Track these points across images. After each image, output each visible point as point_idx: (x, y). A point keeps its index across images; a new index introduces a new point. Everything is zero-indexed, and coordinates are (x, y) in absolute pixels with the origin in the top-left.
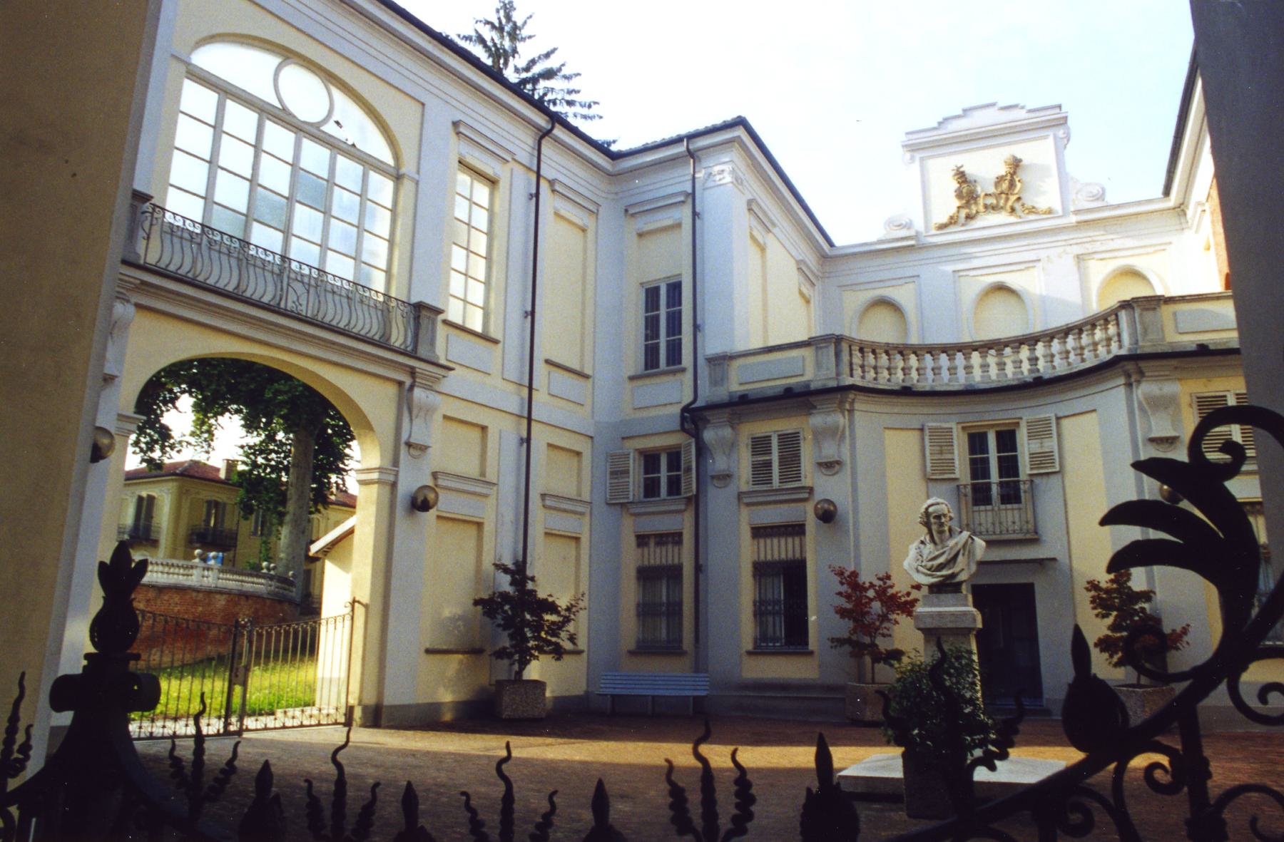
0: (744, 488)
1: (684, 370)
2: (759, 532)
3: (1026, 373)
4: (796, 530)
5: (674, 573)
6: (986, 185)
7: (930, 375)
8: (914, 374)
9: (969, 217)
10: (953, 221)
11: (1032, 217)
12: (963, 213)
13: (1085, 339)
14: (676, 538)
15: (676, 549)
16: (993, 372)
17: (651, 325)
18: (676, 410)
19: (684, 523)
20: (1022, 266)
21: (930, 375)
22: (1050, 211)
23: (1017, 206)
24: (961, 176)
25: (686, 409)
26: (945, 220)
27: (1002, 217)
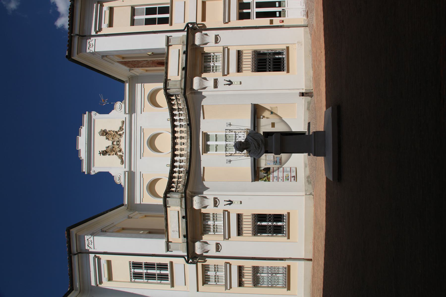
0: (222, 238)
1: (171, 263)
2: (239, 233)
3: (186, 129)
4: (239, 216)
5: (256, 270)
6: (109, 143)
7: (182, 164)
8: (182, 169)
9: (120, 151)
10: (121, 157)
11: (124, 127)
12: (119, 153)
13: (175, 107)
14: (240, 268)
15: (246, 269)
16: (184, 141)
17: (150, 277)
18: (188, 265)
19: (235, 264)
20: (142, 133)
21: (182, 164)
22: (123, 122)
23: (119, 133)
24: (104, 153)
25: (187, 262)
26: (120, 160)
27: (122, 139)
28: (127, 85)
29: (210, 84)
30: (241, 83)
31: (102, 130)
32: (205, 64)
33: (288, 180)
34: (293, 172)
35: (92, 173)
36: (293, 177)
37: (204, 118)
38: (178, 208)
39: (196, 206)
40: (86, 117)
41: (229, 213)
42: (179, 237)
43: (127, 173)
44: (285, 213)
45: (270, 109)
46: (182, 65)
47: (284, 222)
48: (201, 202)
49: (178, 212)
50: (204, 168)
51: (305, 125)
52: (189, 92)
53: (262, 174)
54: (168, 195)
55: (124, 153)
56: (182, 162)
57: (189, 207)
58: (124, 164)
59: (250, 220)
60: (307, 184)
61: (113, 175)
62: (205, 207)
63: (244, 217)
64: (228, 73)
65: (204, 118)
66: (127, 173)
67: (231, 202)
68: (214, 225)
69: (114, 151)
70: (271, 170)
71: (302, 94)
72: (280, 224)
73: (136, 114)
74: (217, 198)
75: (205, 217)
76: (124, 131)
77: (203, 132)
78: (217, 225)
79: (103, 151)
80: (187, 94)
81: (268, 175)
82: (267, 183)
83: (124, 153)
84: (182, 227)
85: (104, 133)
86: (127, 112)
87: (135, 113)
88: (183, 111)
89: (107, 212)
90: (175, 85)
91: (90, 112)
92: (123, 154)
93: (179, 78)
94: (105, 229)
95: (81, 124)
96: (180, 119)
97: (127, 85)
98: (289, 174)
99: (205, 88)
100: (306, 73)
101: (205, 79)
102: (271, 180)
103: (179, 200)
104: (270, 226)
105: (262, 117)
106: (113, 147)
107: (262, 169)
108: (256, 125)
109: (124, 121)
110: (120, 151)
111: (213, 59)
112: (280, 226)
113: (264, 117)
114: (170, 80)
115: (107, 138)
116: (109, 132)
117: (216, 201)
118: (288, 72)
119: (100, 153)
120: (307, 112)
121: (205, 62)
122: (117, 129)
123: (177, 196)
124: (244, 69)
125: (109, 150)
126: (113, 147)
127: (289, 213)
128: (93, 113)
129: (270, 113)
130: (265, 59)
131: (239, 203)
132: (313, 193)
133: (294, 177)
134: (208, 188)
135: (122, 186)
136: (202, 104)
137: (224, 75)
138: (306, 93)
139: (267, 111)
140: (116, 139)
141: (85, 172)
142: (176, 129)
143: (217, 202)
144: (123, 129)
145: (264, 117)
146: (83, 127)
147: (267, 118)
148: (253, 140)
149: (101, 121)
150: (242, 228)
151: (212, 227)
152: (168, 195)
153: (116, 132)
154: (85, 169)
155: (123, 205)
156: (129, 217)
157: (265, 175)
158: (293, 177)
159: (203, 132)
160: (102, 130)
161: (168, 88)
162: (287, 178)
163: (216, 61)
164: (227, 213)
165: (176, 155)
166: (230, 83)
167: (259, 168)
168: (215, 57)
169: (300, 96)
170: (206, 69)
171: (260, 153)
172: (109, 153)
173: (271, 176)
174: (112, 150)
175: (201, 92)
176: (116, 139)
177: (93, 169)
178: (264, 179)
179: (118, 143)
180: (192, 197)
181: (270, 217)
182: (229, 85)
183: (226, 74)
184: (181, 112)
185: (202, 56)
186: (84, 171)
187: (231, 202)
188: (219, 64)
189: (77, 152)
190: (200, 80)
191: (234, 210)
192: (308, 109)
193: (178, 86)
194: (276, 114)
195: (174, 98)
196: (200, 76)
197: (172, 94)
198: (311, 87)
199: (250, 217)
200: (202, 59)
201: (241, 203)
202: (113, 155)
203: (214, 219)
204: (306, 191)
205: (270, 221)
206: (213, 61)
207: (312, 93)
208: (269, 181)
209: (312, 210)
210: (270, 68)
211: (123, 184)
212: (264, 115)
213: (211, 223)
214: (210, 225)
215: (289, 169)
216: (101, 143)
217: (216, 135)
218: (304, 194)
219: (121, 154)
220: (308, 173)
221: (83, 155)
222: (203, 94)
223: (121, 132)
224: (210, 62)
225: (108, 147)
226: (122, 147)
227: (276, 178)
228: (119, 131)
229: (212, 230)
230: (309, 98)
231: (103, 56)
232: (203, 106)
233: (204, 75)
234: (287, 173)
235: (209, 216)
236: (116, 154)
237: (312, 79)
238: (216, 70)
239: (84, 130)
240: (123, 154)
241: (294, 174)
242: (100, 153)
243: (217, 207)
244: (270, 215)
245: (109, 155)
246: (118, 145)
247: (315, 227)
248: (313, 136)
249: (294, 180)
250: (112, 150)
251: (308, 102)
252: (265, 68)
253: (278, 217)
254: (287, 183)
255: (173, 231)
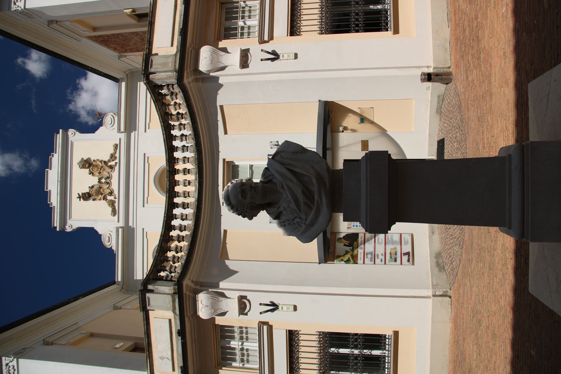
4: (292, 337)
6: (94, 181)
8: (184, 233)
9: (111, 193)
10: (112, 204)
11: (117, 155)
12: (109, 198)
22: (116, 146)
23: (110, 164)
24: (86, 197)
27: (115, 174)
28: (123, 84)
29: (234, 59)
30: (296, 56)
31: (83, 159)
32: (228, 24)
33: (396, 261)
34: (406, 243)
35: (68, 229)
36: (405, 254)
37: (226, 133)
38: (170, 314)
39: (203, 313)
40: (59, 138)
41: (270, 328)
42: (174, 370)
43: (120, 230)
44: (389, 333)
45: (358, 111)
46: (179, 26)
47: (385, 349)
48: (214, 306)
49: (170, 320)
50: (225, 231)
51: (430, 145)
52: (190, 79)
53: (340, 247)
54: (150, 287)
55: (117, 197)
56: (184, 218)
57: (188, 313)
58: (117, 216)
59: (315, 344)
60: (436, 270)
61: (100, 233)
62: (223, 314)
63: (302, 337)
64: (271, 38)
65: (226, 133)
66: (120, 230)
67: (274, 307)
68: (242, 349)
69: (102, 194)
70: (360, 239)
71: (429, 77)
72: (376, 352)
73: (136, 132)
74: (245, 297)
75: (225, 333)
76: (117, 161)
77: (224, 160)
78: (247, 350)
79: (84, 194)
80: (186, 81)
81: (353, 250)
82: (351, 266)
83: (117, 197)
84: (178, 351)
85: (87, 164)
86: (122, 129)
87: (135, 130)
88: (186, 119)
89: (76, 299)
90: (165, 64)
91: (66, 130)
92: (115, 198)
93: (174, 50)
94: (50, 340)
95: (51, 150)
96: (182, 135)
97: (123, 84)
98: (398, 247)
99: (223, 68)
100: (436, 33)
101: (225, 50)
102: (360, 261)
103: (169, 298)
104: (356, 357)
105: (341, 129)
106: (100, 188)
107: (342, 235)
108: (329, 145)
109: (117, 145)
110: (111, 193)
111: (243, 12)
112: (377, 358)
113: (345, 128)
114: (157, 54)
115: (91, 173)
116: (94, 163)
117: (245, 303)
118: (396, 31)
119: (80, 197)
120: (437, 118)
121: (227, 19)
122: (106, 158)
123: (168, 289)
124: (304, 29)
125: (93, 192)
126: (100, 188)
127: (396, 333)
128: (71, 131)
129: (358, 119)
130: (348, 14)
131: (292, 308)
132: (450, 293)
133: (408, 254)
134: (234, 272)
135: (113, 251)
136: (218, 104)
137: (262, 41)
138: (437, 75)
139: (350, 115)
140: (105, 174)
141: (56, 227)
142: (177, 155)
143: (246, 306)
144: (115, 158)
145: (345, 128)
146: (55, 155)
147: (354, 131)
148: (289, 175)
149: (83, 146)
150: (298, 358)
151: (237, 352)
152: (150, 287)
153: (105, 162)
154: (57, 223)
155: (114, 283)
156: (116, 308)
157: (348, 248)
158: (405, 254)
159: (224, 160)
160: (83, 159)
161: (152, 70)
162: (393, 257)
163: (250, 17)
164: (266, 328)
165: (176, 205)
166: (275, 56)
167: (335, 233)
168: (247, 9)
169: (423, 80)
170: (229, 33)
171: (312, 224)
172: (93, 197)
173: (360, 251)
174: (99, 192)
175: (217, 78)
176: (105, 174)
177: (69, 222)
178: (346, 258)
179: (108, 180)
180: (197, 292)
181: (356, 340)
182: (273, 60)
183: (266, 38)
184: (183, 121)
185: (221, 8)
186: (55, 225)
187: (274, 307)
188: (254, 22)
189: (46, 195)
190: (213, 53)
191: (281, 322)
192: (439, 111)
193: (171, 67)
194: (372, 123)
195: (164, 91)
196: (216, 45)
197: (159, 83)
198: (446, 62)
199: (315, 338)
200: (221, 13)
201: (295, 308)
202: (100, 199)
203: (241, 338)
204: (434, 286)
205: (356, 347)
206: (243, 18)
207: (450, 74)
208: (355, 262)
209: (447, 329)
210: (357, 25)
211: (114, 248)
212: (345, 123)
213: (235, 344)
214: (234, 349)
215: (396, 238)
216: (82, 181)
217: (251, 167)
218: (430, 293)
219: (111, 198)
220: (437, 247)
221: (54, 200)
222: (220, 82)
223: (113, 163)
224: (236, 18)
225: (93, 187)
226: (115, 186)
227: (369, 256)
228: (109, 161)
229: (238, 358)
230: (440, 87)
231: (51, 22)
232: (222, 107)
233: (222, 44)
234: (393, 247)
235: (233, 332)
236: (105, 198)
237: (448, 46)
238: (249, 33)
239: (56, 160)
240: (115, 198)
241: (407, 248)
242: (80, 197)
243: (246, 314)
244: (356, 334)
245: (94, 200)
246: (108, 183)
247: (455, 368)
248: (515, 161)
249: (409, 261)
250: (99, 192)
251: (439, 97)
252: (348, 26)
253: (375, 341)
254: (393, 268)
255: (162, 358)
